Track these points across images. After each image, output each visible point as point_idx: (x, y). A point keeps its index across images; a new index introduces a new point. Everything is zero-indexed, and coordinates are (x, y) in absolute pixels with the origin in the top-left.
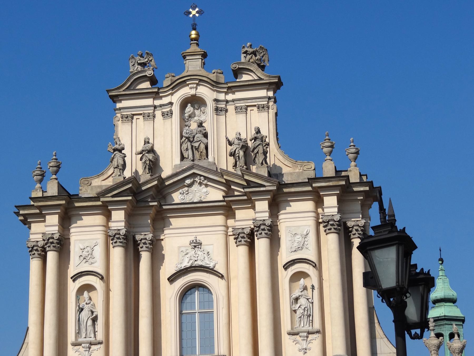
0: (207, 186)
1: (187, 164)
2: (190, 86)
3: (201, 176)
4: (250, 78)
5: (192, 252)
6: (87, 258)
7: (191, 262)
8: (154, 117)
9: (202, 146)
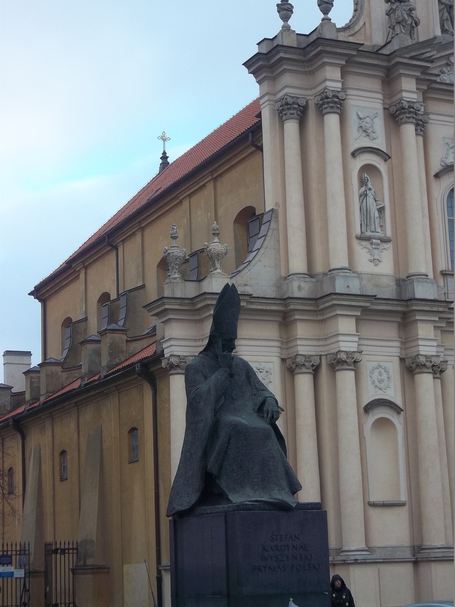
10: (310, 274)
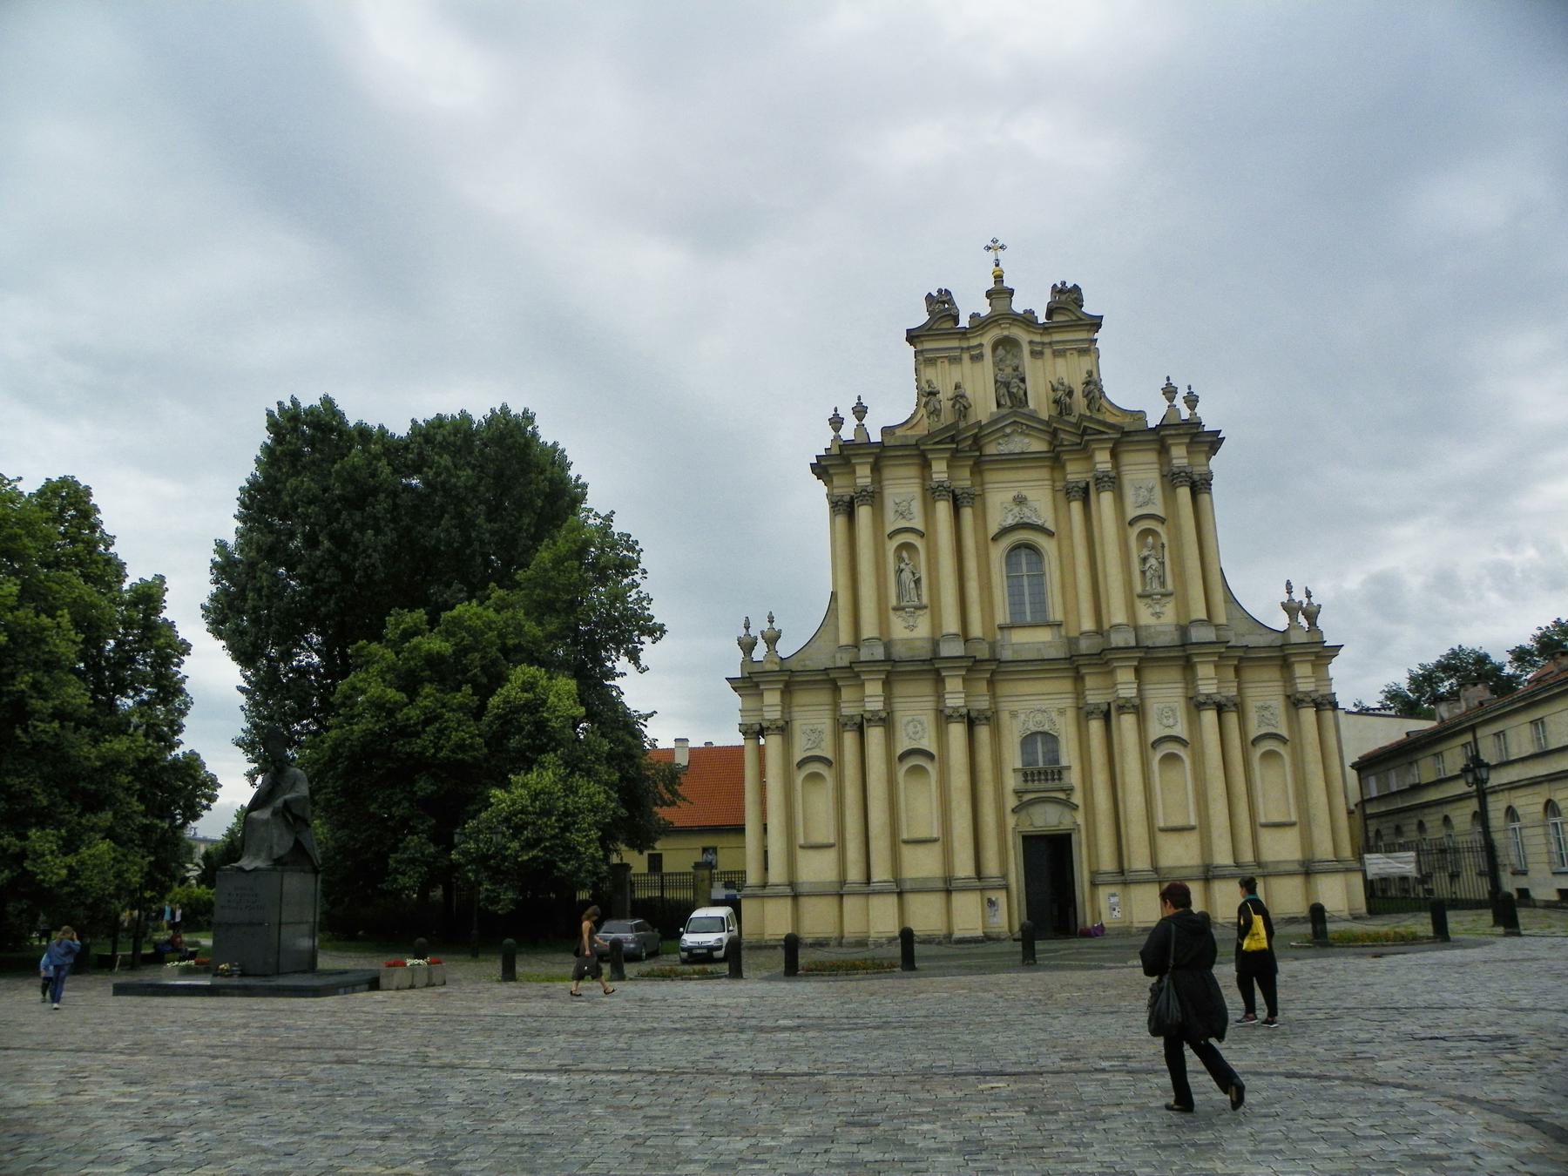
0: (1028, 435)
1: (1005, 411)
3: (1022, 424)
4: (1067, 319)
5: (1017, 509)
8: (961, 359)
9: (1022, 392)
10: (856, 645)
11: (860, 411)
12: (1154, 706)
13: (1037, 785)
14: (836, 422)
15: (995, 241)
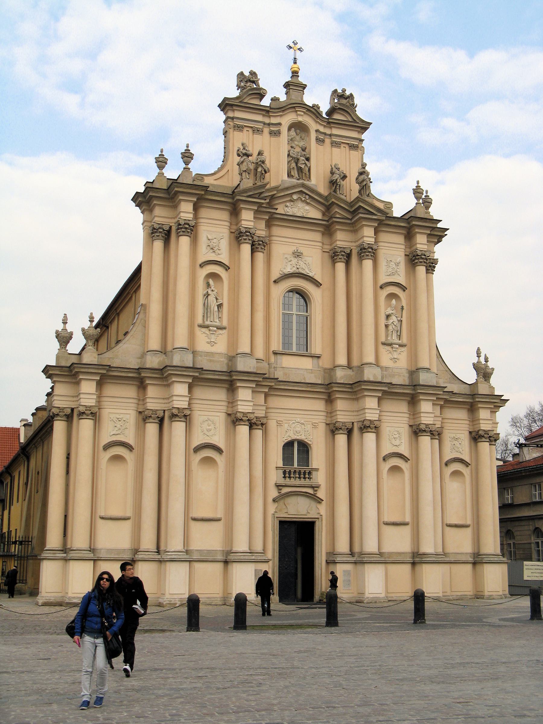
0: (308, 204)
1: (294, 181)
2: (298, 112)
3: (307, 194)
5: (294, 261)
6: (214, 249)
7: (295, 269)
10: (164, 351)
11: (187, 156)
12: (386, 429)
13: (292, 482)
14: (161, 162)
15: (295, 43)
